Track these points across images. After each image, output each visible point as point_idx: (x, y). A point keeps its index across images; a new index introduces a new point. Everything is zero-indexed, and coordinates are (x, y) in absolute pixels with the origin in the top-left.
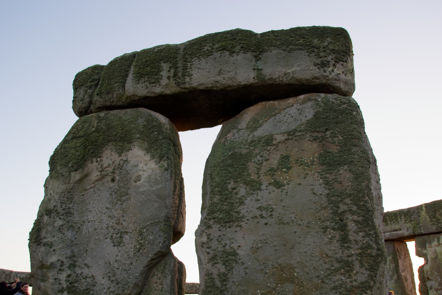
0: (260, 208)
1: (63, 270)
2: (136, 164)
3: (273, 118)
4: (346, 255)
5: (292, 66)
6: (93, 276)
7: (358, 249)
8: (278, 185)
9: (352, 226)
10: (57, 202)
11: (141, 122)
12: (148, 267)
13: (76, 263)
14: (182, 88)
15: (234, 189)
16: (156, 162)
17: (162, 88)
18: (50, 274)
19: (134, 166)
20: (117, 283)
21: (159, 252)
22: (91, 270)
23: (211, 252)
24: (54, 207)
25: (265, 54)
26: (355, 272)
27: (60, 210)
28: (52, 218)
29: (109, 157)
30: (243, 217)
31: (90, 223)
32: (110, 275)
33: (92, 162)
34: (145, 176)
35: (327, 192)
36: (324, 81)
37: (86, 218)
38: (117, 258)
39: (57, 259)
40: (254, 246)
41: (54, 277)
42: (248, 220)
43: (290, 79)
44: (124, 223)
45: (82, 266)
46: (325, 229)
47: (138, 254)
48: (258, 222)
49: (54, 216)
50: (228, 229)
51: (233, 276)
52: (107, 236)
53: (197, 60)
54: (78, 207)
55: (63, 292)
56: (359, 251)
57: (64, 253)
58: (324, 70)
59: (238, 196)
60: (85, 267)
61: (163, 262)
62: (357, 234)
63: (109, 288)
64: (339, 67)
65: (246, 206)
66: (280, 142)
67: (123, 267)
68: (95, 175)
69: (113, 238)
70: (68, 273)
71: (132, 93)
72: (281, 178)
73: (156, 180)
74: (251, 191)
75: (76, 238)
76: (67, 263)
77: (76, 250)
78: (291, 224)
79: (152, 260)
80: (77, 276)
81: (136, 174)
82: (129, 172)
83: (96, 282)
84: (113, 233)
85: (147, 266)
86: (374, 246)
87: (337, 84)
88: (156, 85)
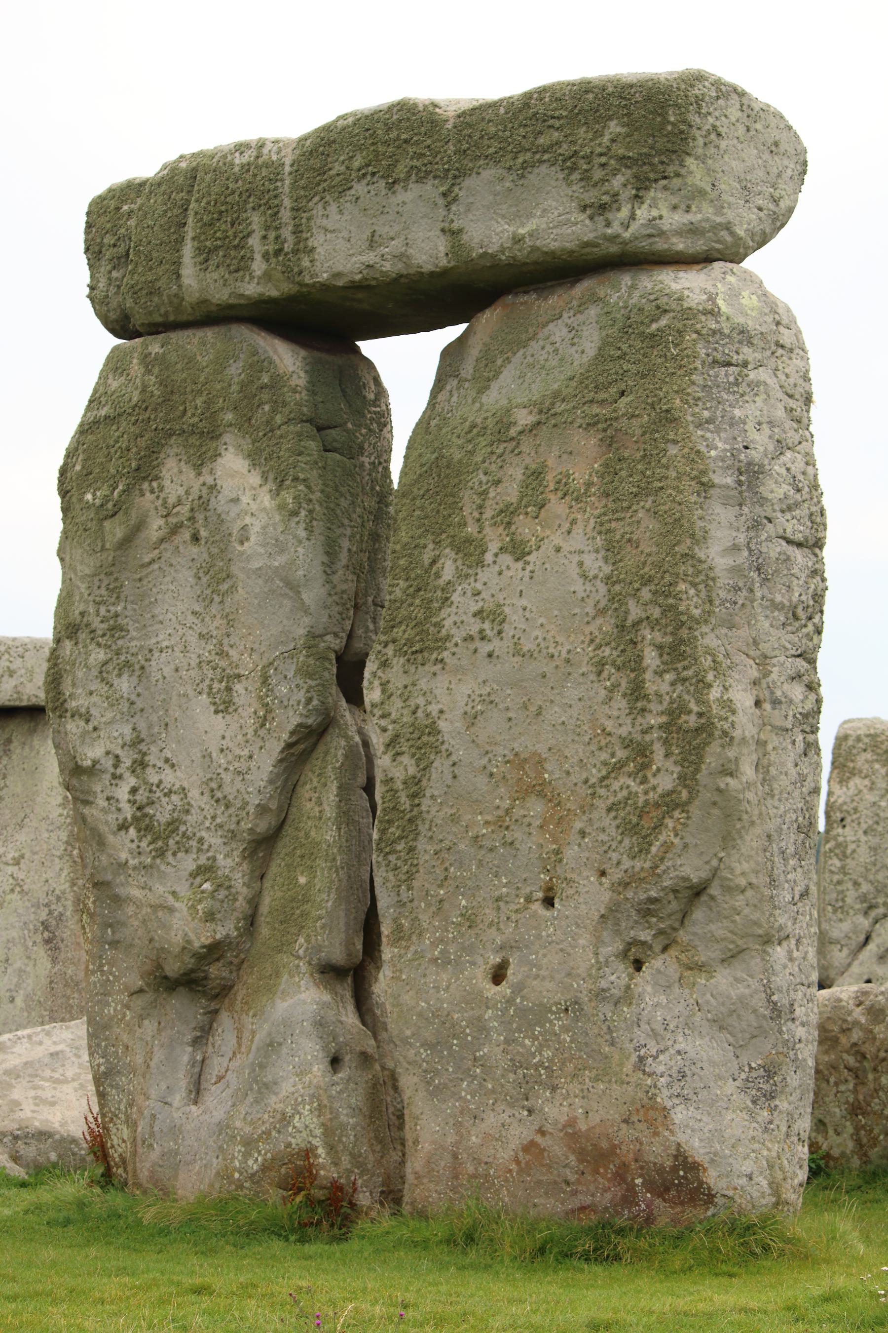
0: (478, 614)
1: (120, 777)
2: (234, 496)
3: (522, 351)
4: (640, 728)
5: (530, 216)
6: (184, 789)
7: (662, 713)
8: (518, 550)
9: (651, 659)
10: (87, 602)
11: (235, 370)
12: (284, 764)
13: (147, 758)
14: (299, 284)
15: (434, 562)
16: (271, 491)
17: (258, 284)
18: (98, 788)
19: (232, 500)
20: (227, 807)
21: (300, 725)
22: (178, 773)
23: (390, 727)
24: (82, 614)
25: (468, 182)
26: (654, 767)
27: (96, 623)
28: (80, 646)
29: (176, 478)
30: (448, 637)
31: (164, 655)
32: (214, 785)
33: (143, 495)
34: (256, 527)
35: (607, 569)
36: (614, 249)
37: (154, 641)
38: (224, 742)
39: (103, 750)
40: (468, 709)
41: (105, 795)
42: (456, 645)
43: (529, 253)
44: (232, 652)
45: (159, 764)
46: (600, 666)
47: (262, 732)
48: (476, 651)
49: (84, 641)
50: (420, 668)
51: (431, 783)
52: (201, 686)
53: (321, 205)
54: (135, 610)
55: (127, 828)
56: (664, 719)
57: (116, 734)
58: (607, 220)
59: (441, 582)
60: (166, 767)
61: (321, 748)
62: (661, 676)
63: (214, 818)
64: (654, 199)
65: (454, 607)
66: (521, 433)
67: (237, 765)
68: (156, 526)
69: (215, 690)
70: (132, 784)
71: (197, 295)
72: (527, 531)
73: (277, 540)
74: (466, 570)
75: (139, 695)
77: (142, 725)
78: (535, 655)
79: (289, 746)
80: (151, 791)
81: (239, 524)
82: (223, 516)
83: (189, 804)
84: (212, 680)
85: (281, 761)
86: (693, 706)
87: (660, 245)
88: (243, 277)
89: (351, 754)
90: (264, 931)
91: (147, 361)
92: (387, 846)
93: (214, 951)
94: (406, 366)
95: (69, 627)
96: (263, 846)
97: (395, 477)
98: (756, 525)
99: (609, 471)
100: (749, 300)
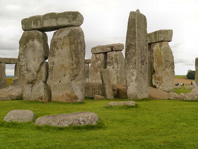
8: (62, 48)
9: (74, 57)
11: (36, 34)
29: (31, 42)
68: (28, 46)
76: (26, 65)
89: (46, 64)
90: (38, 79)
91: (28, 33)
92: (50, 72)
93: (34, 80)
94: (50, 35)
95: (20, 54)
96: (38, 72)
97: (49, 44)
98: (82, 47)
99: (70, 42)
100: (81, 30)
